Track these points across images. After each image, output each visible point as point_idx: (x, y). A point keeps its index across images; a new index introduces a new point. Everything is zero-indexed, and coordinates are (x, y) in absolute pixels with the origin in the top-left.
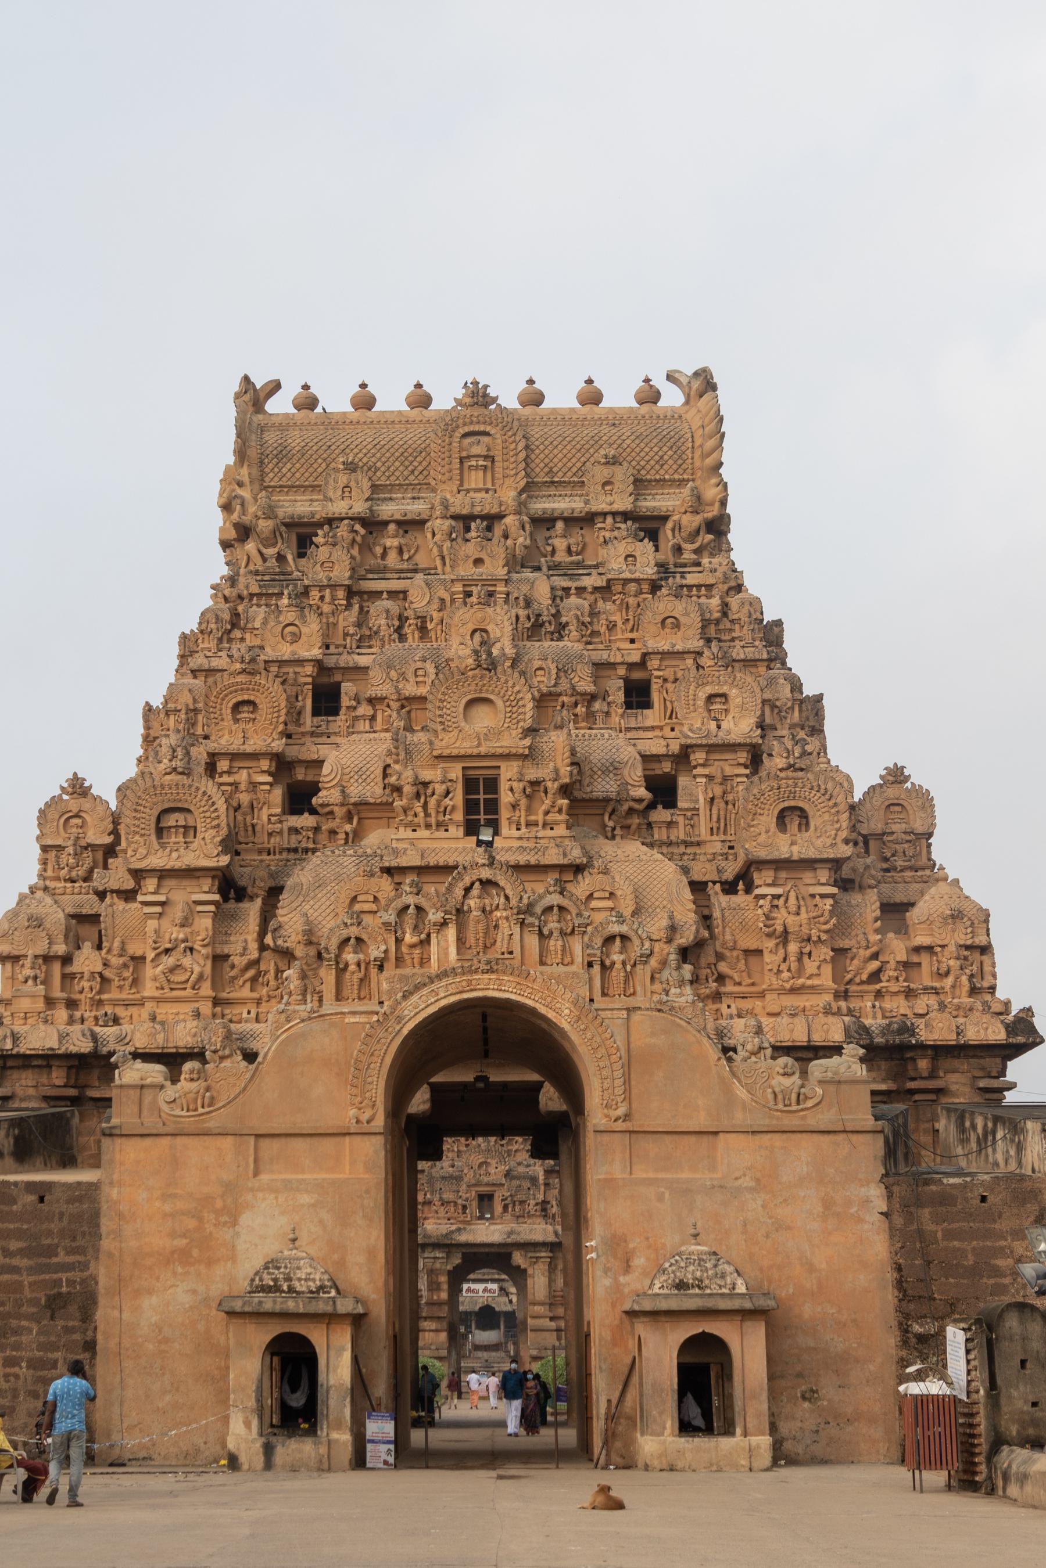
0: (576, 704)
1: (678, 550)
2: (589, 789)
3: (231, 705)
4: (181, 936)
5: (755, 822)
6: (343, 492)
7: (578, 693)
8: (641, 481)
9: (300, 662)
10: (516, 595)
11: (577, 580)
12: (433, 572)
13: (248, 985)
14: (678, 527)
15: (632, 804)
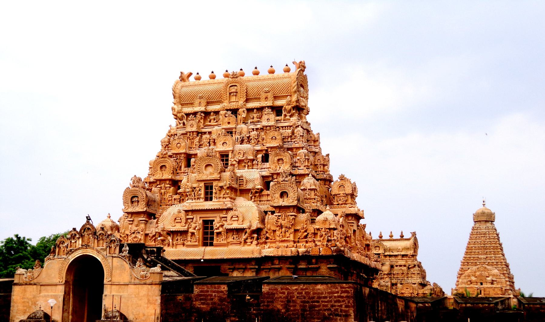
0: (248, 162)
1: (285, 116)
2: (245, 186)
3: (160, 166)
4: (136, 229)
5: (274, 196)
6: (199, 104)
7: (249, 159)
8: (276, 97)
9: (181, 154)
10: (238, 132)
11: (257, 126)
12: (219, 126)
13: (154, 241)
14: (285, 109)
15: (256, 190)
